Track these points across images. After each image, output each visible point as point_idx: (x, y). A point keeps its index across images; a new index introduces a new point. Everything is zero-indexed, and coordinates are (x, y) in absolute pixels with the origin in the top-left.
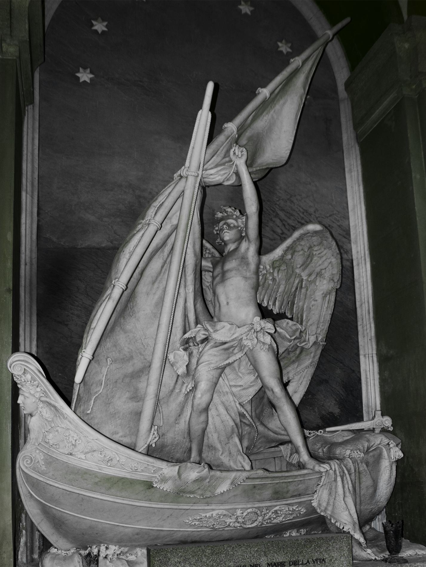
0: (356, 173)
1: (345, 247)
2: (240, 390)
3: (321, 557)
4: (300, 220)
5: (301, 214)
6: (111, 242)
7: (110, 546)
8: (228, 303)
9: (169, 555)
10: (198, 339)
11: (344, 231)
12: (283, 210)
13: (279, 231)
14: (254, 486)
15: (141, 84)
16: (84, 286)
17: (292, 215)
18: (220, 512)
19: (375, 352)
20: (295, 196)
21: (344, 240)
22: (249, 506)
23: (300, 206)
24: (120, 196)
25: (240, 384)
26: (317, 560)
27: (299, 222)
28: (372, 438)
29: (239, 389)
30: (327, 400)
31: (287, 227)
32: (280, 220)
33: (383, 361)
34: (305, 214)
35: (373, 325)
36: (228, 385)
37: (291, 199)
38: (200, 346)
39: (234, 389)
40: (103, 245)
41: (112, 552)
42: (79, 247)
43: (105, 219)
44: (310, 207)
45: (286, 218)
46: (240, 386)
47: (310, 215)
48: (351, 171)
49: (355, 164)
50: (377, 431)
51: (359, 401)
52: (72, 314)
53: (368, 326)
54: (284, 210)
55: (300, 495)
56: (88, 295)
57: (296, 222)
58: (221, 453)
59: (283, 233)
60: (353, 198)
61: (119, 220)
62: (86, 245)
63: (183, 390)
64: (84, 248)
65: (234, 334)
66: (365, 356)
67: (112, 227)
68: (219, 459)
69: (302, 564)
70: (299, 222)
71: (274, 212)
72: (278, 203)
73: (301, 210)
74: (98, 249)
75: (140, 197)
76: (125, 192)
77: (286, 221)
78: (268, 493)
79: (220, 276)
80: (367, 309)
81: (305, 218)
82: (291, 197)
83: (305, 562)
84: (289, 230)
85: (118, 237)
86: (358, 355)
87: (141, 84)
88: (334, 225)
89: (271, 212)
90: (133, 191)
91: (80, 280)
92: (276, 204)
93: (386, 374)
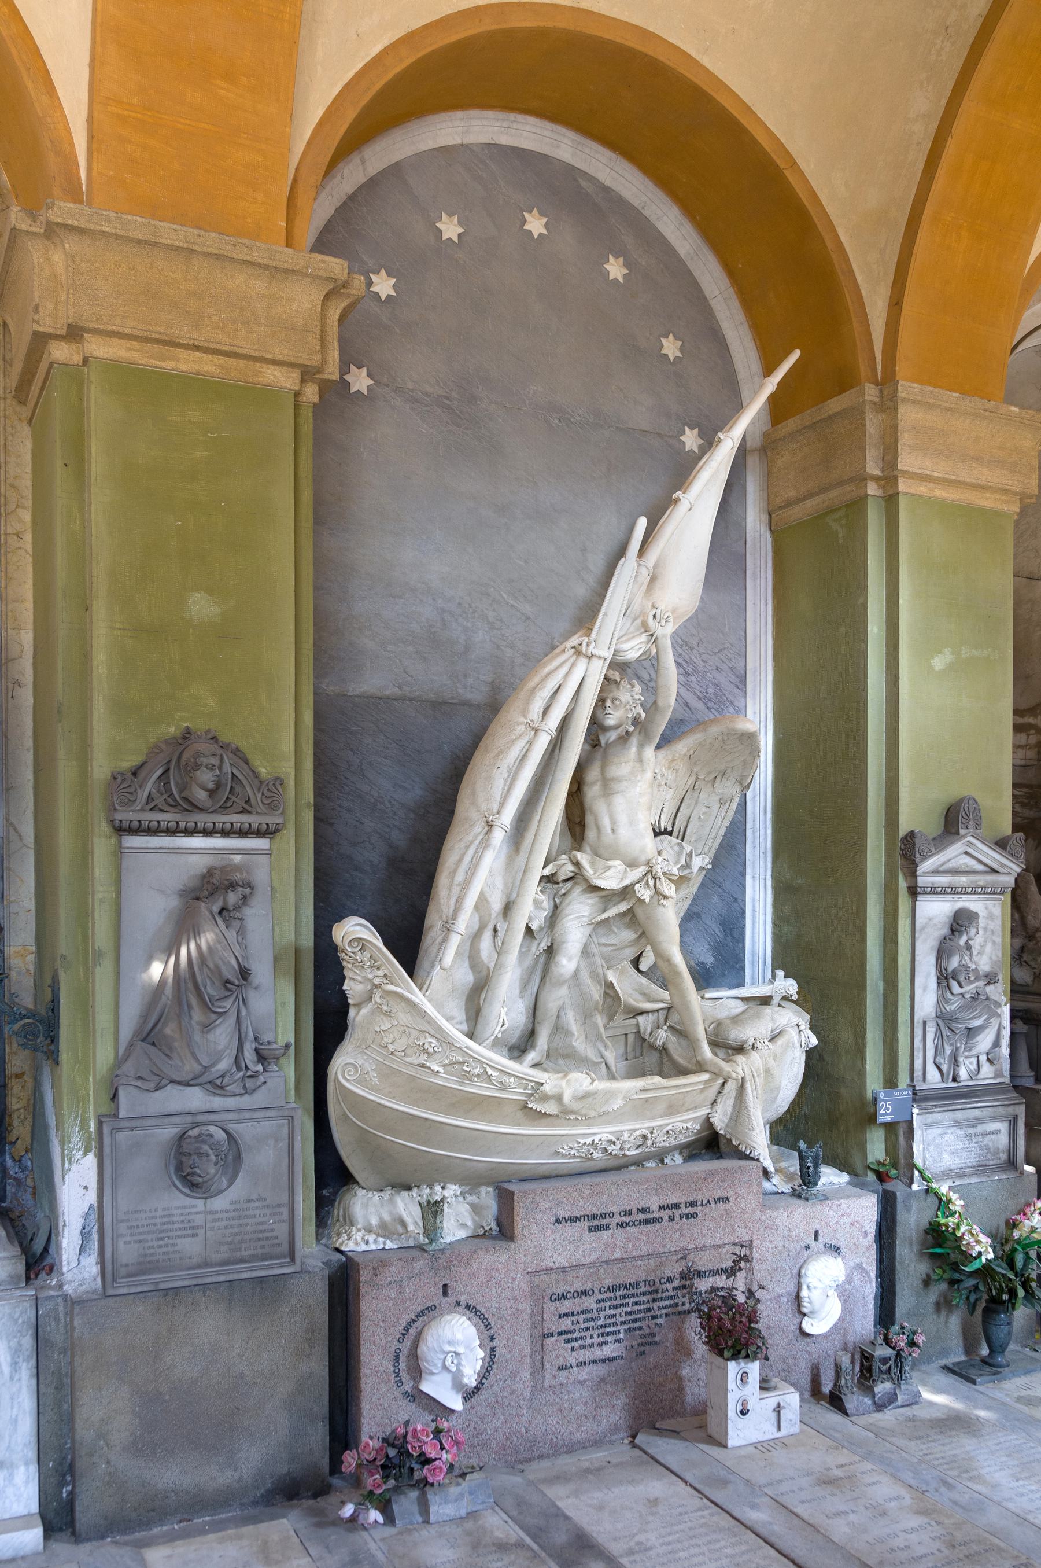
0: (763, 581)
1: (736, 703)
3: (724, 1195)
5: (678, 648)
6: (400, 688)
7: (448, 1185)
8: (613, 830)
9: (537, 1198)
10: (562, 877)
11: (737, 677)
13: (647, 677)
14: (647, 1100)
15: (448, 402)
18: (604, 1137)
19: (769, 872)
21: (737, 691)
22: (637, 1126)
24: (413, 608)
25: (613, 942)
26: (719, 1199)
28: (776, 1016)
29: (611, 948)
33: (783, 891)
35: (769, 832)
38: (561, 885)
39: (604, 949)
40: (387, 693)
41: (452, 1193)
43: (390, 647)
44: (693, 635)
46: (612, 945)
47: (692, 649)
48: (755, 579)
49: (763, 567)
50: (776, 1000)
51: (740, 945)
52: (340, 806)
53: (762, 832)
55: (696, 1108)
56: (363, 775)
59: (650, 680)
60: (755, 623)
61: (411, 649)
63: (534, 949)
66: (754, 876)
68: (573, 1046)
69: (702, 1205)
73: (679, 641)
75: (443, 610)
78: (661, 1107)
79: (599, 783)
80: (762, 804)
83: (704, 1202)
86: (744, 875)
87: (448, 402)
88: (724, 667)
90: (433, 599)
91: (351, 750)
93: (787, 910)
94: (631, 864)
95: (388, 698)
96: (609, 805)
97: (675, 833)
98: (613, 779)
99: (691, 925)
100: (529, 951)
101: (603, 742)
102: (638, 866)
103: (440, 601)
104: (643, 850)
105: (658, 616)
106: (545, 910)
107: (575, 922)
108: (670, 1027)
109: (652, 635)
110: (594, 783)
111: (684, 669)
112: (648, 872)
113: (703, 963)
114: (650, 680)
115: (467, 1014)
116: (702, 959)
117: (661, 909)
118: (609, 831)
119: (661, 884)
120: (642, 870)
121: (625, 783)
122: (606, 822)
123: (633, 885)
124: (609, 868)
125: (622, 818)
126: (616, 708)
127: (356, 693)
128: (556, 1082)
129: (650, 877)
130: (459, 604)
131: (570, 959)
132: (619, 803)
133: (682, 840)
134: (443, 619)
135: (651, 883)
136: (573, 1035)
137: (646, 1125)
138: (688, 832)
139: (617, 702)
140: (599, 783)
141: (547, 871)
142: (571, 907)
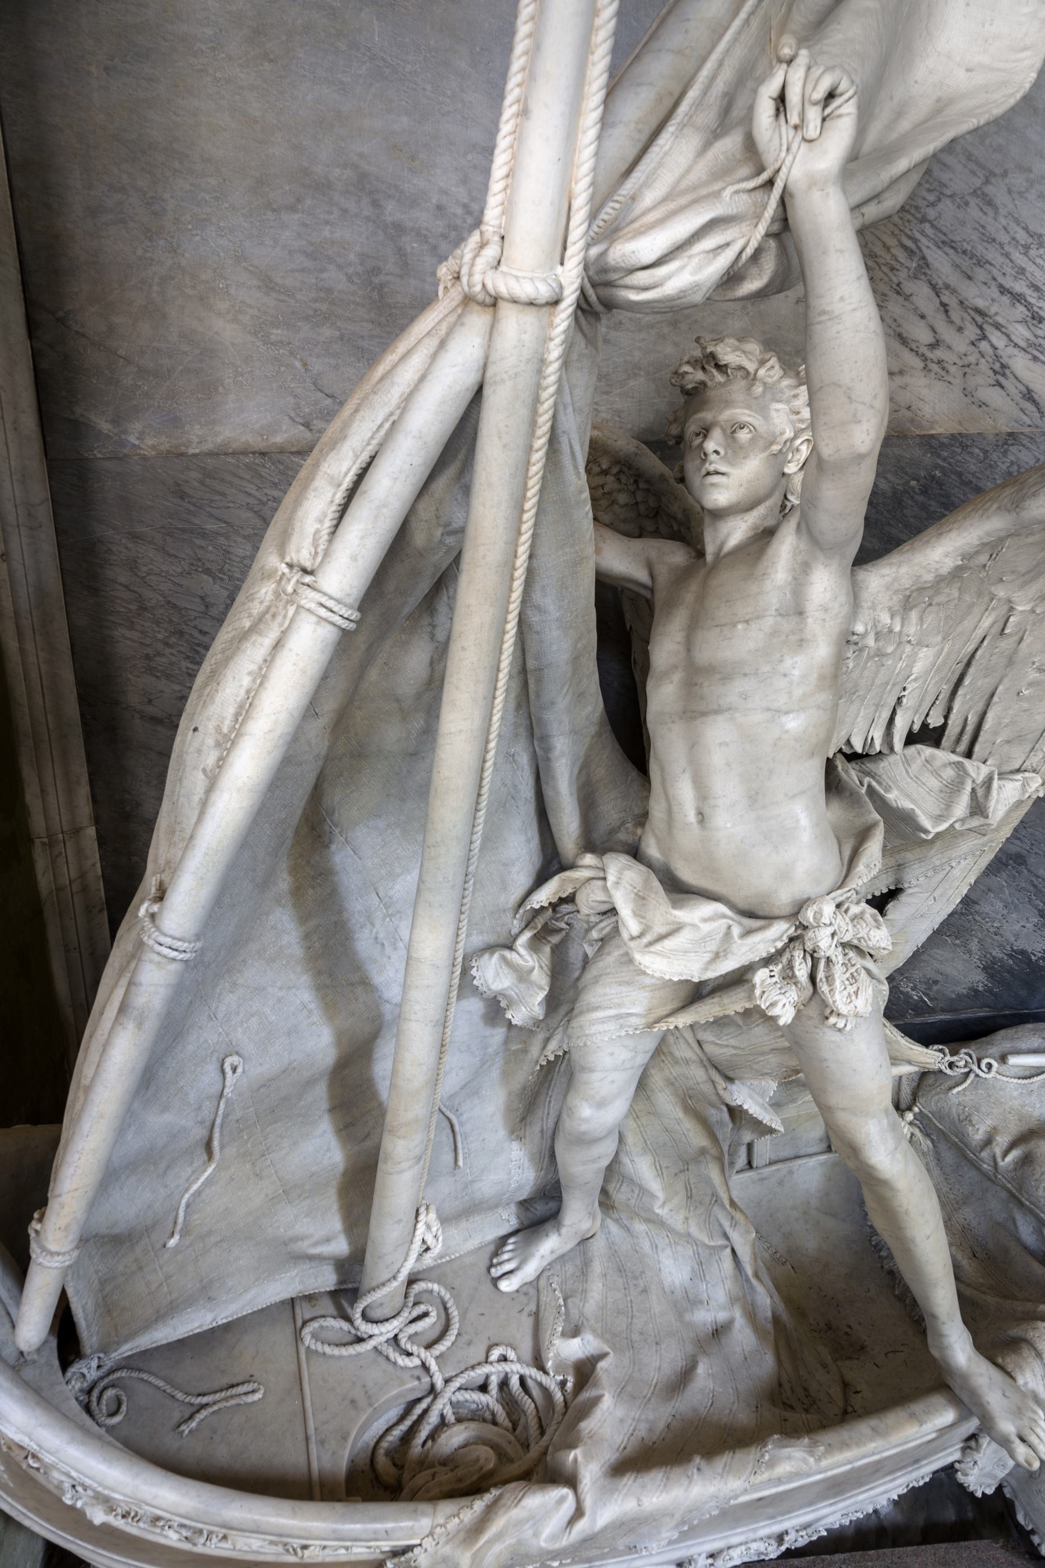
4: (1008, 283)
8: (702, 817)
12: (947, 244)
16: (225, 593)
17: (981, 262)
20: (1005, 174)
23: (1017, 221)
24: (326, 232)
27: (1003, 290)
30: (1014, 916)
31: (956, 314)
32: (934, 287)
34: (1033, 253)
37: (989, 190)
40: (279, 439)
42: (191, 451)
45: (953, 278)
54: (951, 244)
57: (995, 292)
58: (659, 1203)
59: (935, 345)
61: (327, 332)
62: (219, 440)
64: (212, 454)
65: (717, 956)
67: (305, 365)
70: (1003, 290)
71: (911, 253)
72: (932, 213)
73: (1022, 236)
74: (263, 454)
75: (399, 228)
76: (345, 211)
77: (954, 291)
81: (1030, 268)
82: (987, 182)
84: (960, 329)
85: (329, 401)
89: (901, 255)
90: (375, 204)
91: (208, 571)
92: (924, 220)
94: (754, 915)
95: (282, 451)
96: (694, 745)
97: (952, 731)
98: (710, 670)
99: (1000, 880)
100: (525, 1051)
101: (710, 549)
102: (770, 918)
103: (390, 206)
104: (785, 875)
105: (794, 97)
106: (541, 988)
107: (611, 1026)
108: (921, 1117)
109: (770, 183)
110: (666, 674)
111: (1028, 306)
113: (1023, 952)
114: (935, 345)
115: (344, 1223)
116: (1020, 945)
117: (831, 1036)
118: (692, 817)
119: (829, 979)
120: (779, 932)
121: (740, 685)
122: (685, 792)
125: (727, 788)
126: (735, 451)
127: (208, 446)
128: (447, 1550)
129: (798, 954)
130: (439, 208)
131: (601, 1104)
132: (719, 735)
133: (969, 754)
134: (400, 252)
135: (802, 971)
136: (653, 1196)
137: (767, 1531)
138: (987, 725)
139: (743, 436)
140: (677, 677)
141: (543, 896)
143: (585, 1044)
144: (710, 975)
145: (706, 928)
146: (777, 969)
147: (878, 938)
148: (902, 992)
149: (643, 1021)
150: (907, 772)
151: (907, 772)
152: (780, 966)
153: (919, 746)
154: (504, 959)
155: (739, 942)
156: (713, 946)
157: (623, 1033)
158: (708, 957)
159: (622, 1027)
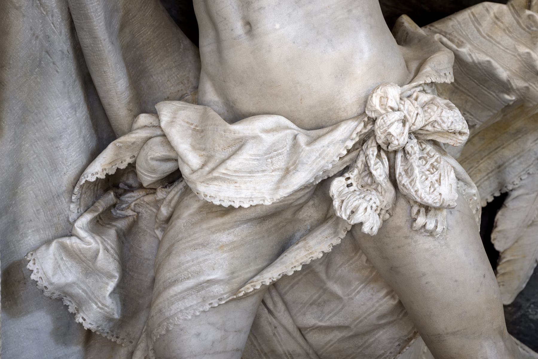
2: (342, 340)
25: (336, 320)
36: (291, 327)
46: (339, 328)
65: (287, 172)
94: (318, 125)
102: (336, 124)
106: (111, 277)
107: (192, 301)
112: (363, 141)
117: (424, 243)
119: (409, 172)
120: (347, 133)
123: (320, 189)
124: (240, 144)
129: (372, 151)
135: (380, 171)
141: (98, 169)
142: (174, 261)
143: (168, 331)
144: (283, 193)
145: (269, 139)
146: (353, 175)
147: (451, 119)
148: (531, 320)
149: (227, 288)
150: (479, 31)
151: (479, 31)
152: (356, 172)
153: (486, 4)
154: (64, 248)
155: (308, 148)
156: (281, 163)
157: (207, 307)
158: (277, 175)
159: (204, 300)
